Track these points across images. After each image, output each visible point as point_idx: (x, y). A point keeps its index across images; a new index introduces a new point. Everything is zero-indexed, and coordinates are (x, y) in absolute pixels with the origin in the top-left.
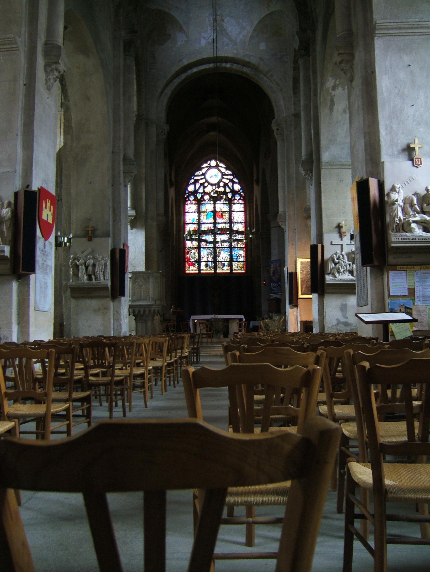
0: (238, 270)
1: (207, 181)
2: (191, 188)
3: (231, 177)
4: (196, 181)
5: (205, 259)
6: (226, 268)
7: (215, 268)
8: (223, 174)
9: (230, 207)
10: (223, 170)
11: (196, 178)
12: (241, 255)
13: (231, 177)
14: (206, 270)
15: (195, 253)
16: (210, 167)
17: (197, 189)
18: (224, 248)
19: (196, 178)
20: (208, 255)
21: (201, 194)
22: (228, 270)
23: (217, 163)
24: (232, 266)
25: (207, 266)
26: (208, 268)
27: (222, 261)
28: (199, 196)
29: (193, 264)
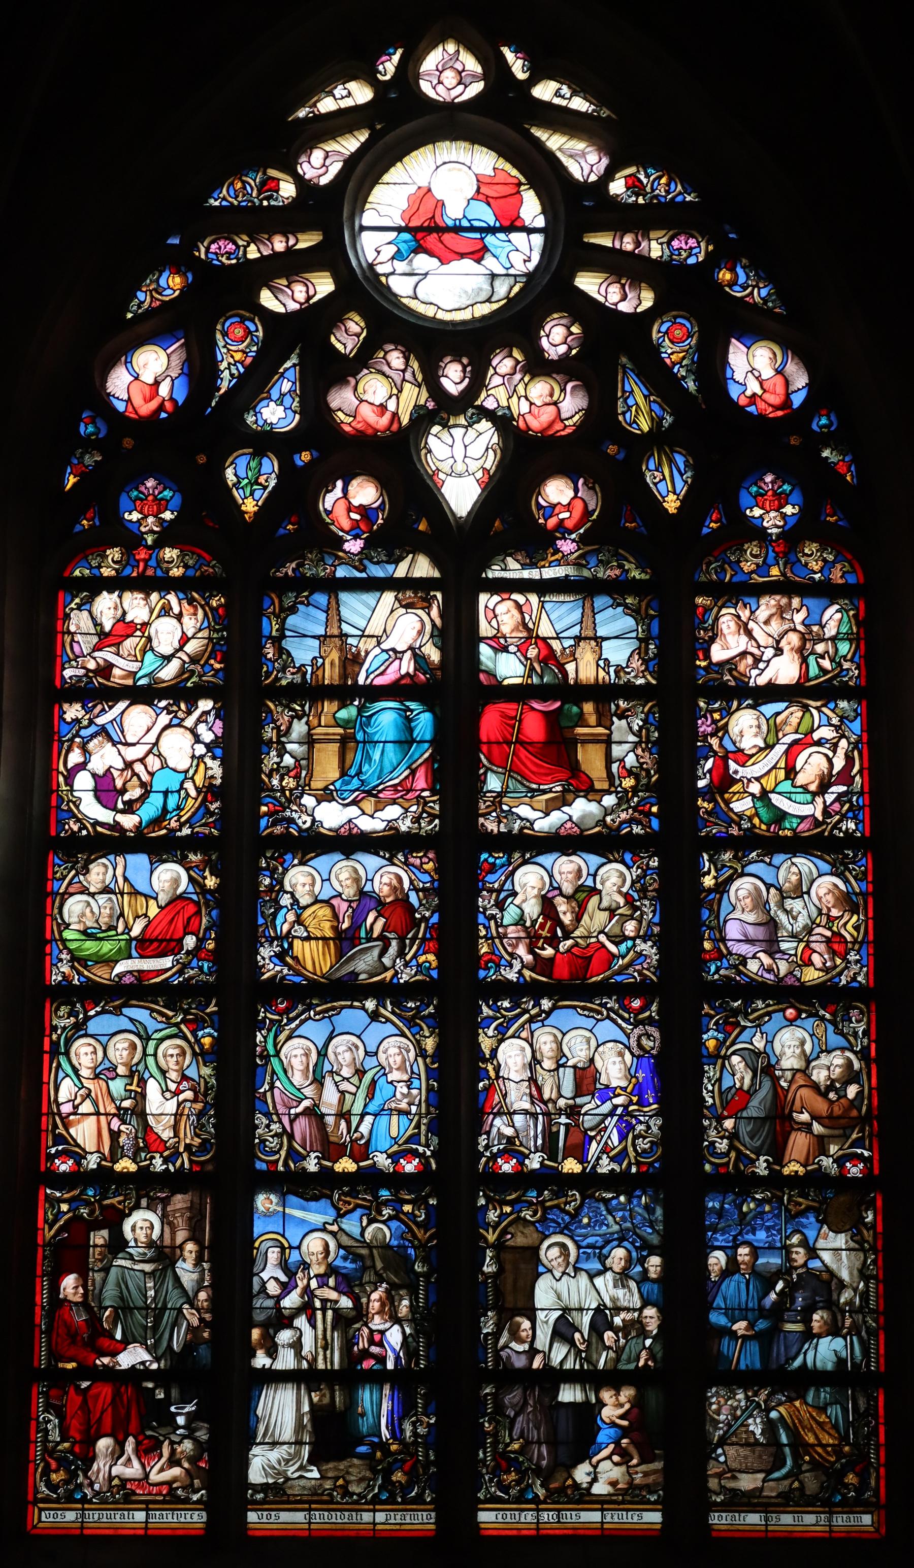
0: (790, 1500)
1: (362, 291)
2: (146, 375)
3: (693, 250)
4: (229, 291)
5: (304, 1342)
6: (602, 1473)
7: (451, 1470)
8: (574, 211)
9: (675, 640)
10: (582, 160)
11: (217, 250)
12: (824, 1285)
13: (693, 250)
14: (313, 1499)
15: (164, 1256)
16: (402, 122)
17: (225, 383)
18: (589, 1182)
19: (217, 250)
20: (348, 1284)
21: (270, 467)
22: (628, 1496)
23: (495, 70)
24: (704, 1450)
25: (330, 1434)
26: (356, 1469)
27: (554, 1377)
28: (249, 483)
29: (137, 1412)
